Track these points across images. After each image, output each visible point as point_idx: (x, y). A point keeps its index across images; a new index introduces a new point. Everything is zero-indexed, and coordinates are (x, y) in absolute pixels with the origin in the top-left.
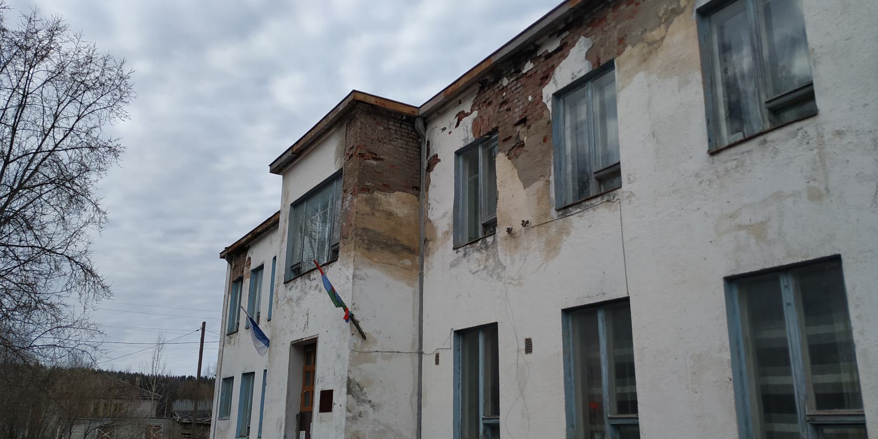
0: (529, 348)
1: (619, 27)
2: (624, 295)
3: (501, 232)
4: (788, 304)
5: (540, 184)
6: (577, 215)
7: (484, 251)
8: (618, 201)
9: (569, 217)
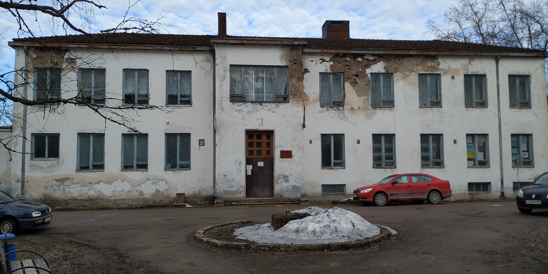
0: (358, 142)
1: (395, 65)
2: (394, 133)
3: (346, 107)
5: (365, 97)
7: (338, 111)
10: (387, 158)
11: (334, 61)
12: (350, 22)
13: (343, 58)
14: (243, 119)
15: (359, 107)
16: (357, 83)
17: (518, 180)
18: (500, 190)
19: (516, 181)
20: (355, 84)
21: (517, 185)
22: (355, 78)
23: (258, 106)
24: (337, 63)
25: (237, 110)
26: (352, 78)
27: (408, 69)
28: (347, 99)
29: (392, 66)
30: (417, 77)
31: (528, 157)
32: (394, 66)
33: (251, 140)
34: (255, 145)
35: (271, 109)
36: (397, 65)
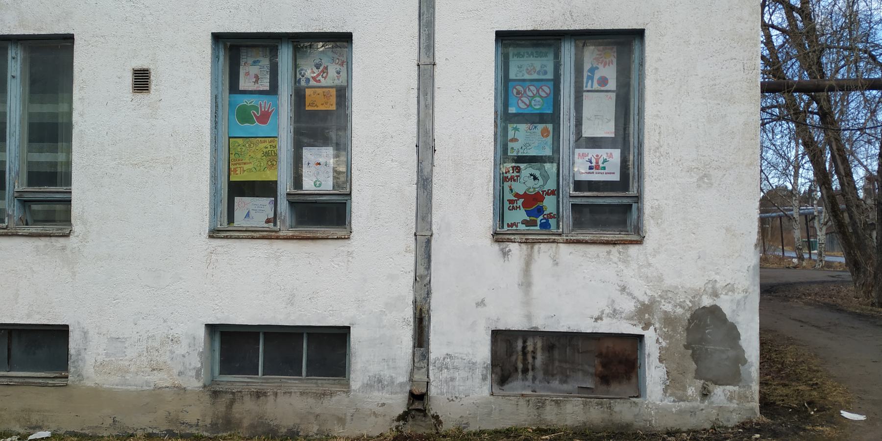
4: (13, 77)
17: (529, 317)
18: (403, 378)
19: (515, 322)
21: (524, 348)
31: (616, 177)
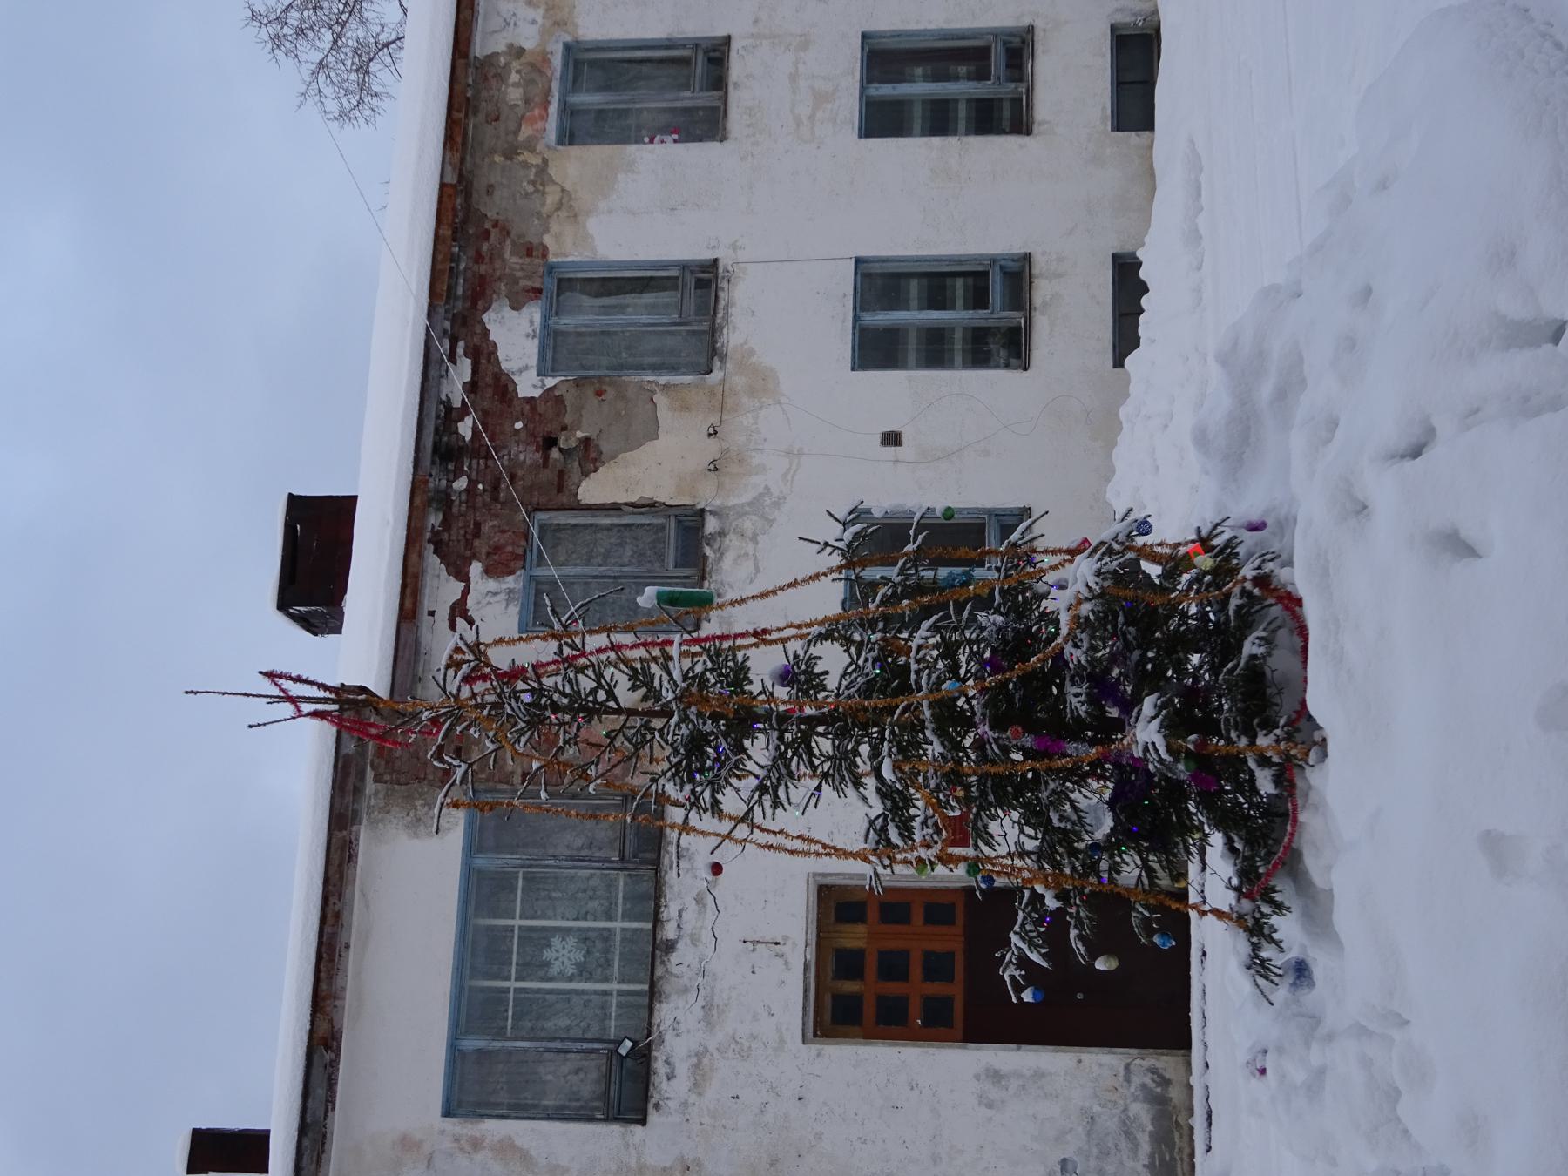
0: (892, 439)
1: (507, 255)
3: (706, 495)
6: (730, 334)
7: (727, 541)
8: (735, 265)
9: (729, 350)
10: (979, 299)
11: (464, 557)
12: (295, 493)
13: (455, 510)
14: (744, 1054)
15: (710, 435)
16: (586, 441)
20: (593, 455)
22: (561, 450)
23: (682, 960)
24: (477, 543)
25: (697, 1087)
26: (559, 466)
27: (527, 195)
28: (666, 492)
29: (513, 269)
30: (575, 151)
32: (514, 260)
33: (869, 1010)
34: (893, 988)
35: (696, 892)
36: (508, 247)
